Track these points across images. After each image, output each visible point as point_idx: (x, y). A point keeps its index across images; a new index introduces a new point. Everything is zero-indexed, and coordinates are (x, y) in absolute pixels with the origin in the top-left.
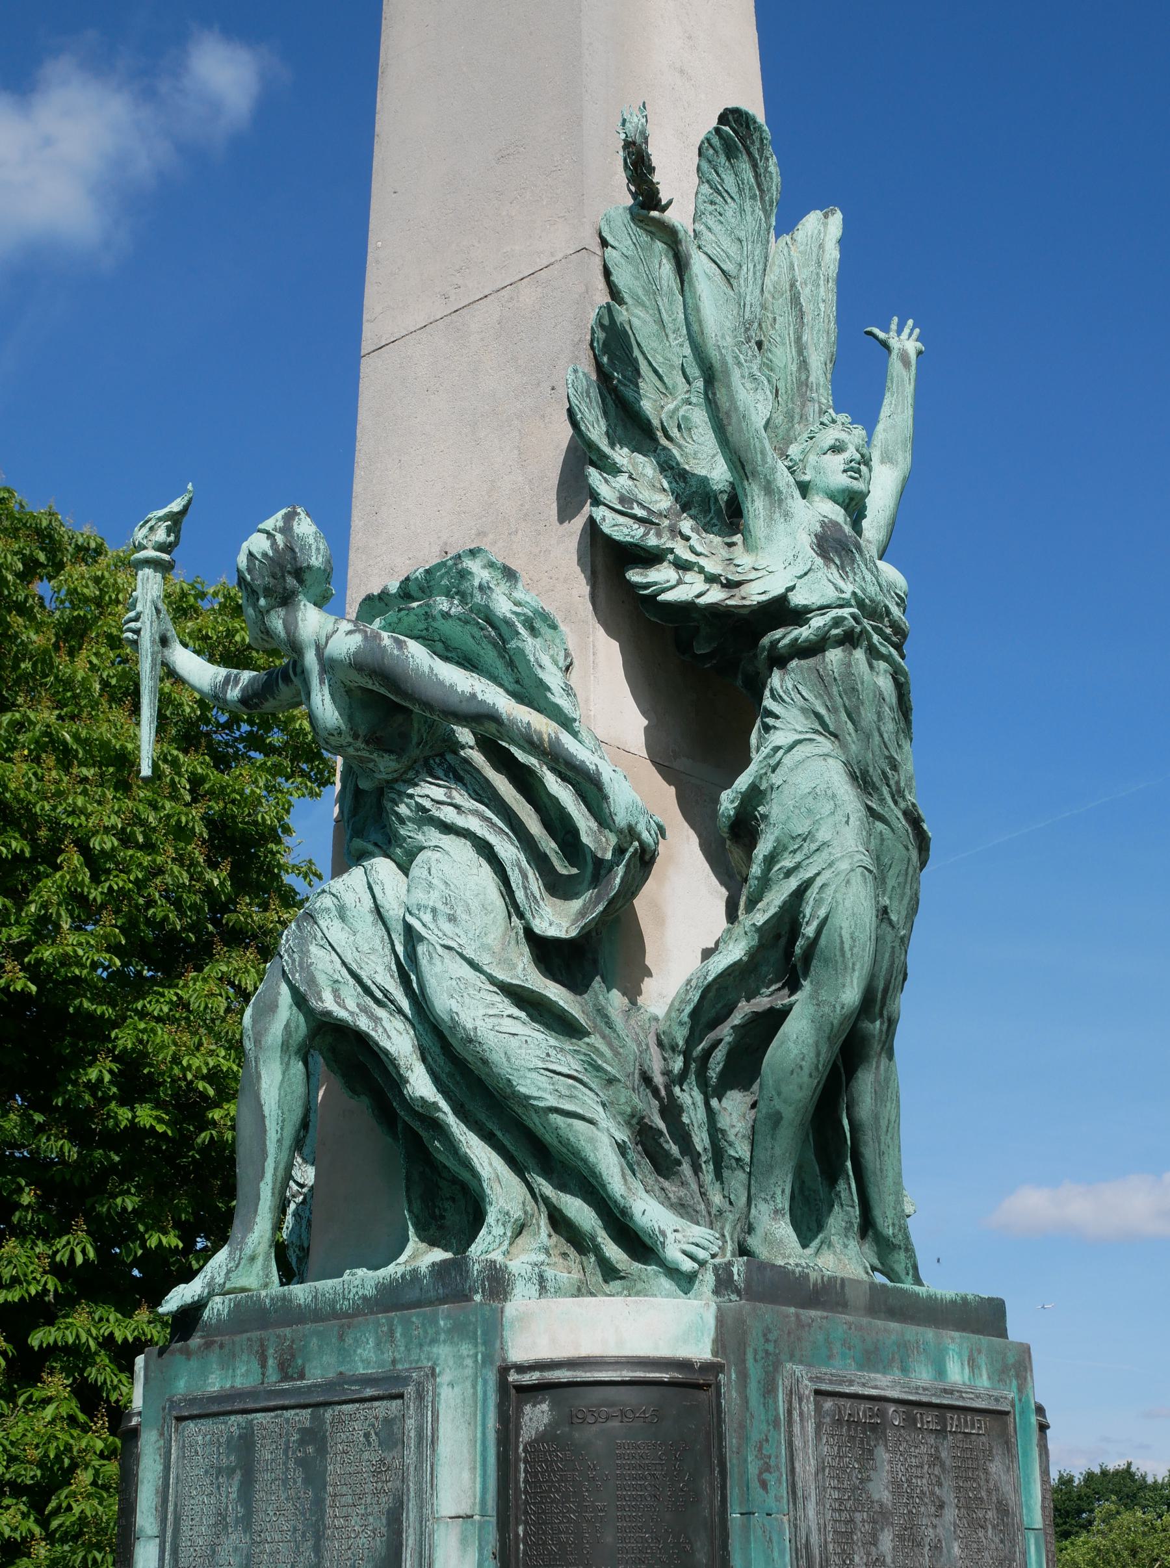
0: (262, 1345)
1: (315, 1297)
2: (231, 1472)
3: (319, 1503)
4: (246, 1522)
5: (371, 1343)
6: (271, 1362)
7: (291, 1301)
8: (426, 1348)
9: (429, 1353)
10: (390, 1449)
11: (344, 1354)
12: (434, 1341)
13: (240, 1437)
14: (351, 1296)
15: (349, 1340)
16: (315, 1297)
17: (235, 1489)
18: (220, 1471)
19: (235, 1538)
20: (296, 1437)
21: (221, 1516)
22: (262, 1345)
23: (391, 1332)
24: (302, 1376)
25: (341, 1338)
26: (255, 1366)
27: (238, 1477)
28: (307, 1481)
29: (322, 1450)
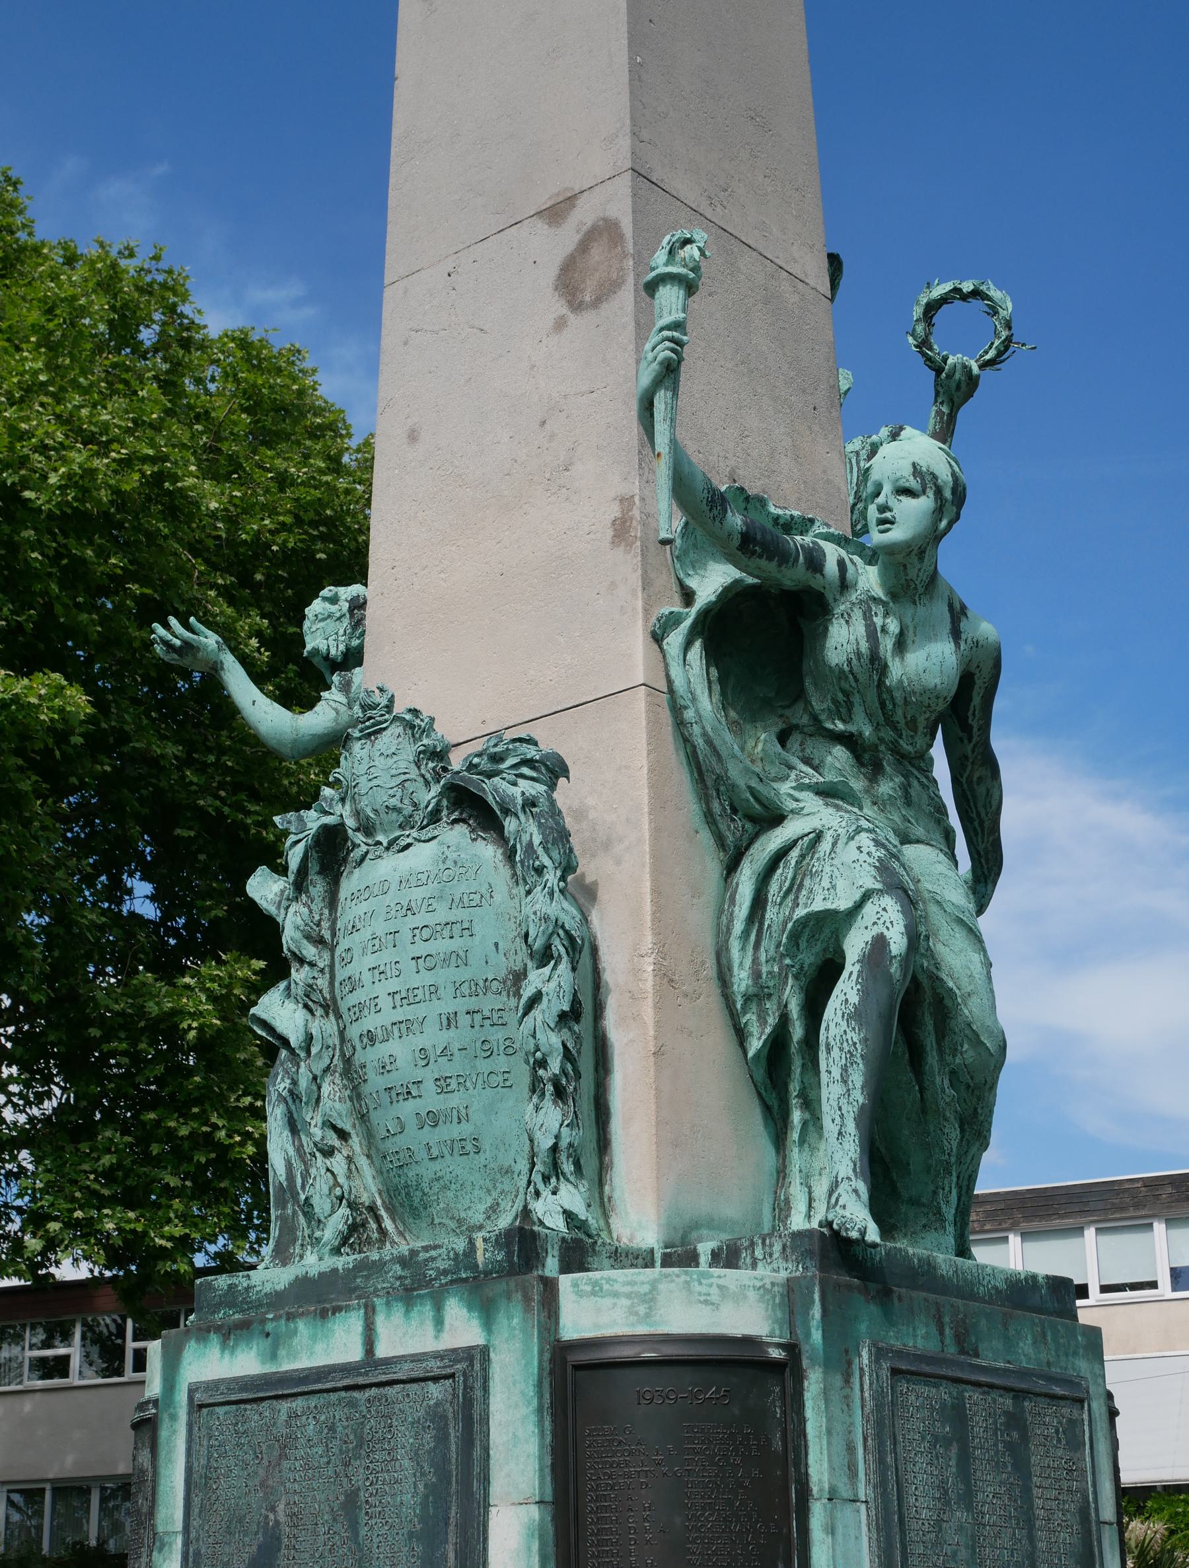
0: (938, 1310)
1: (956, 1272)
2: (947, 1443)
3: (1027, 1491)
4: (968, 1499)
5: (1029, 1341)
6: (947, 1331)
7: (935, 1268)
8: (1070, 1358)
9: (1073, 1364)
10: (1076, 1451)
11: (1010, 1344)
12: (1075, 1354)
13: (953, 1407)
14: (985, 1283)
15: (1012, 1332)
16: (956, 1272)
17: (953, 1463)
18: (936, 1440)
19: (961, 1515)
20: (1002, 1420)
21: (943, 1488)
22: (938, 1310)
23: (1044, 1335)
24: (977, 1355)
25: (1005, 1326)
26: (934, 1331)
27: (954, 1450)
28: (1015, 1466)
29: (1025, 1438)
